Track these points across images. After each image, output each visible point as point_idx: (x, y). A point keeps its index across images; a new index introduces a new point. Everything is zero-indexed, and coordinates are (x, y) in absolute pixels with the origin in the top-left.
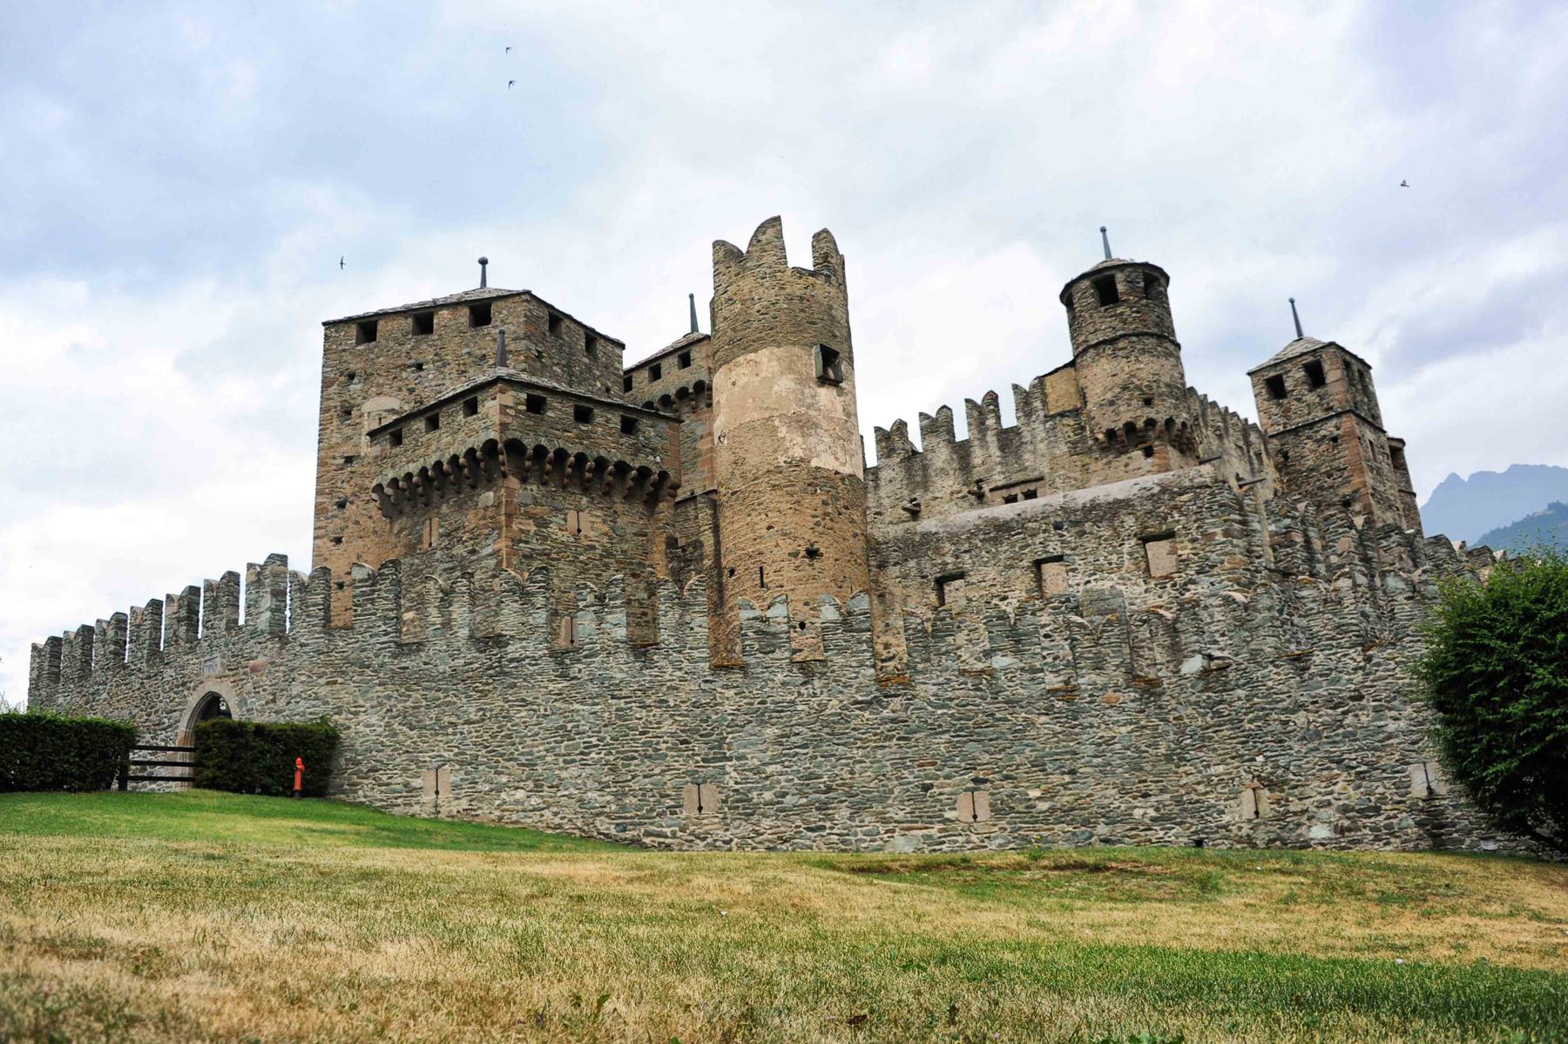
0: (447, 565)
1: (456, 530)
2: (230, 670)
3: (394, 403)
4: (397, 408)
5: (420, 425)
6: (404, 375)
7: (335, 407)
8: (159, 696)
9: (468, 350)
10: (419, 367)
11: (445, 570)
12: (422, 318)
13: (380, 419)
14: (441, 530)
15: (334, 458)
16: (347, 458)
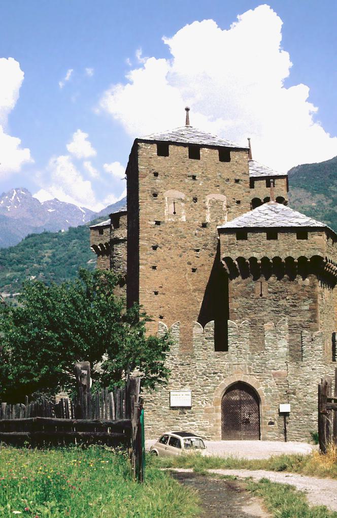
0: (274, 309)
1: (281, 292)
2: (255, 372)
3: (183, 196)
4: (183, 199)
5: (264, 234)
6: (186, 181)
7: (148, 191)
8: (193, 376)
9: (220, 174)
10: (194, 177)
11: (272, 311)
12: (194, 151)
13: (174, 203)
14: (269, 290)
15: (150, 221)
16: (156, 221)
